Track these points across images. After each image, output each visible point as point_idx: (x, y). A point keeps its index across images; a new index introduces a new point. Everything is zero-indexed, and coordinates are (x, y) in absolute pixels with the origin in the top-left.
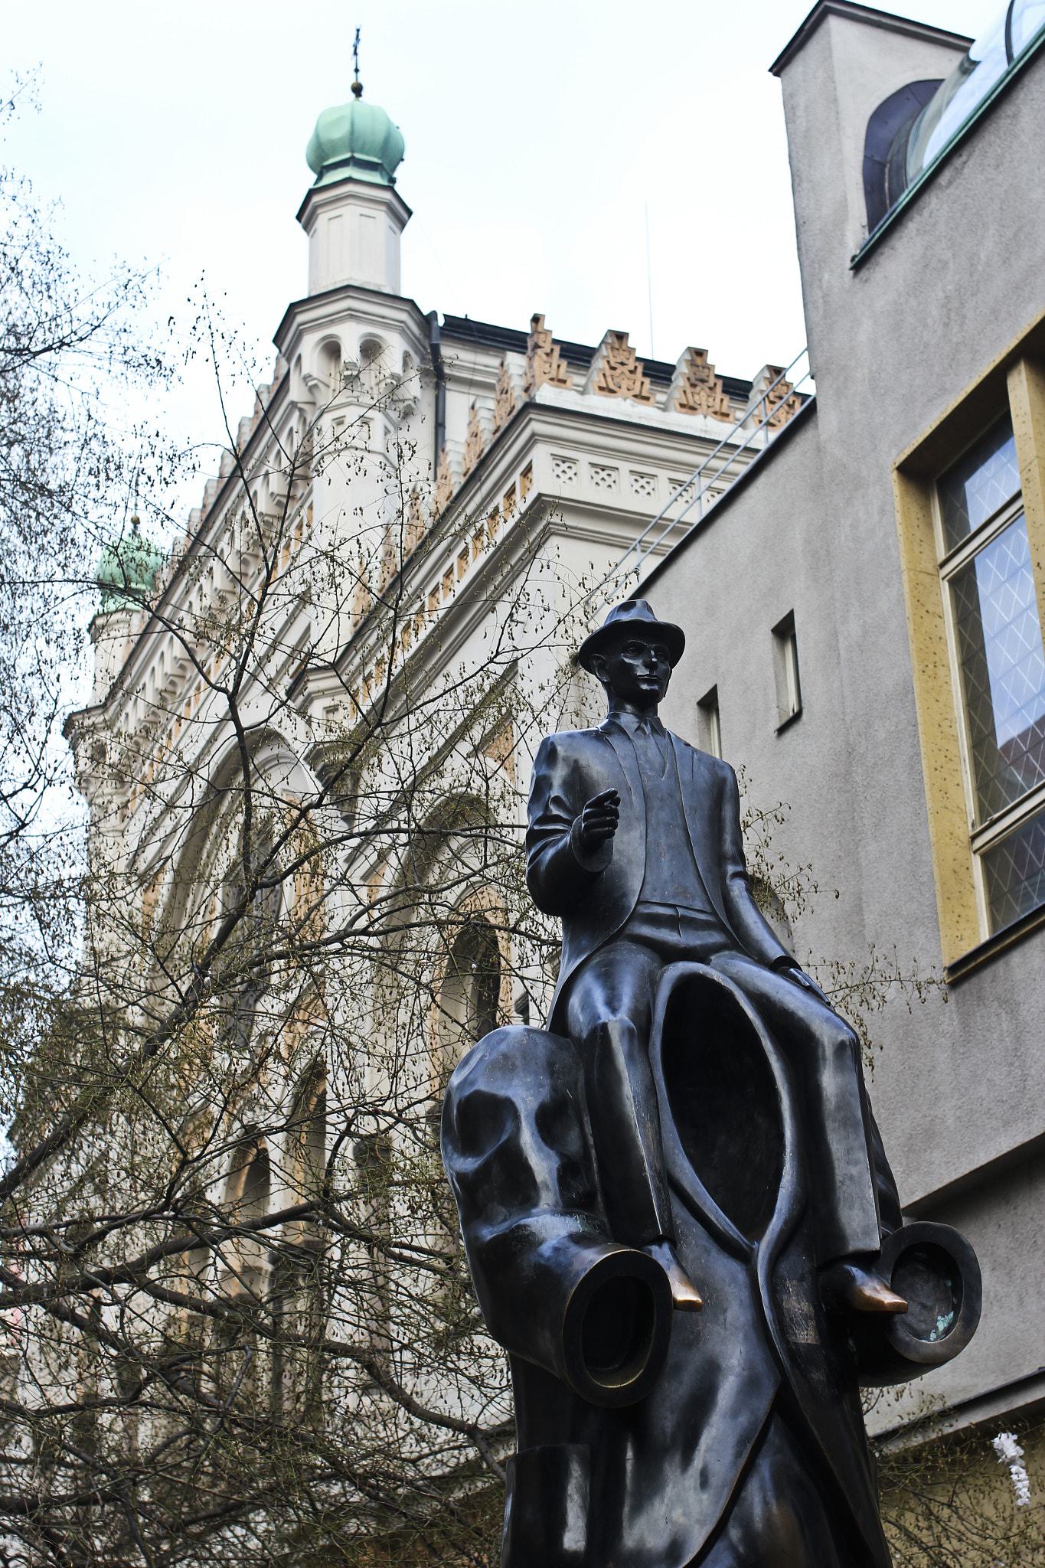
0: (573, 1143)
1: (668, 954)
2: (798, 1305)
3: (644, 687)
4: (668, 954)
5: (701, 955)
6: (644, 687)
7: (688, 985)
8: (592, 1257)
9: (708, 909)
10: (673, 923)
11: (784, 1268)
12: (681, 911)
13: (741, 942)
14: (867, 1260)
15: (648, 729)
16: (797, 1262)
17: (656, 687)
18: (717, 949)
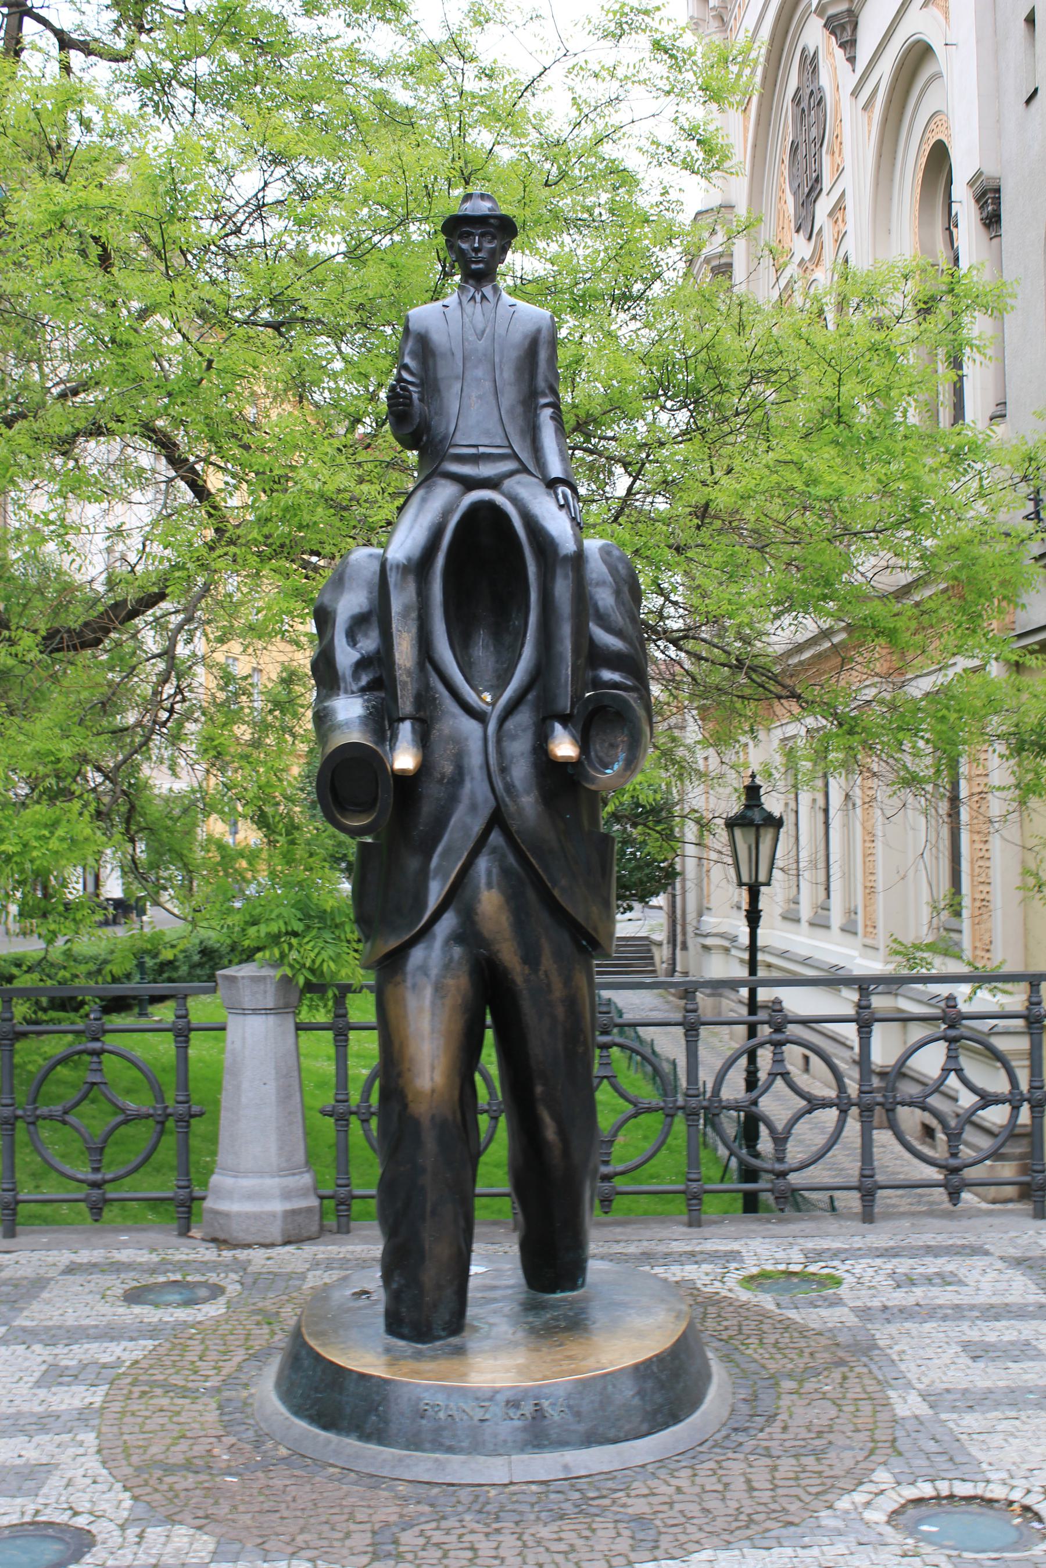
0: (369, 643)
1: (469, 484)
2: (520, 747)
3: (473, 266)
4: (469, 484)
5: (492, 483)
6: (473, 266)
7: (477, 508)
8: (356, 736)
9: (506, 444)
10: (475, 459)
11: (510, 724)
12: (482, 450)
13: (533, 463)
14: (565, 720)
15: (478, 297)
16: (524, 718)
17: (481, 266)
18: (511, 474)
